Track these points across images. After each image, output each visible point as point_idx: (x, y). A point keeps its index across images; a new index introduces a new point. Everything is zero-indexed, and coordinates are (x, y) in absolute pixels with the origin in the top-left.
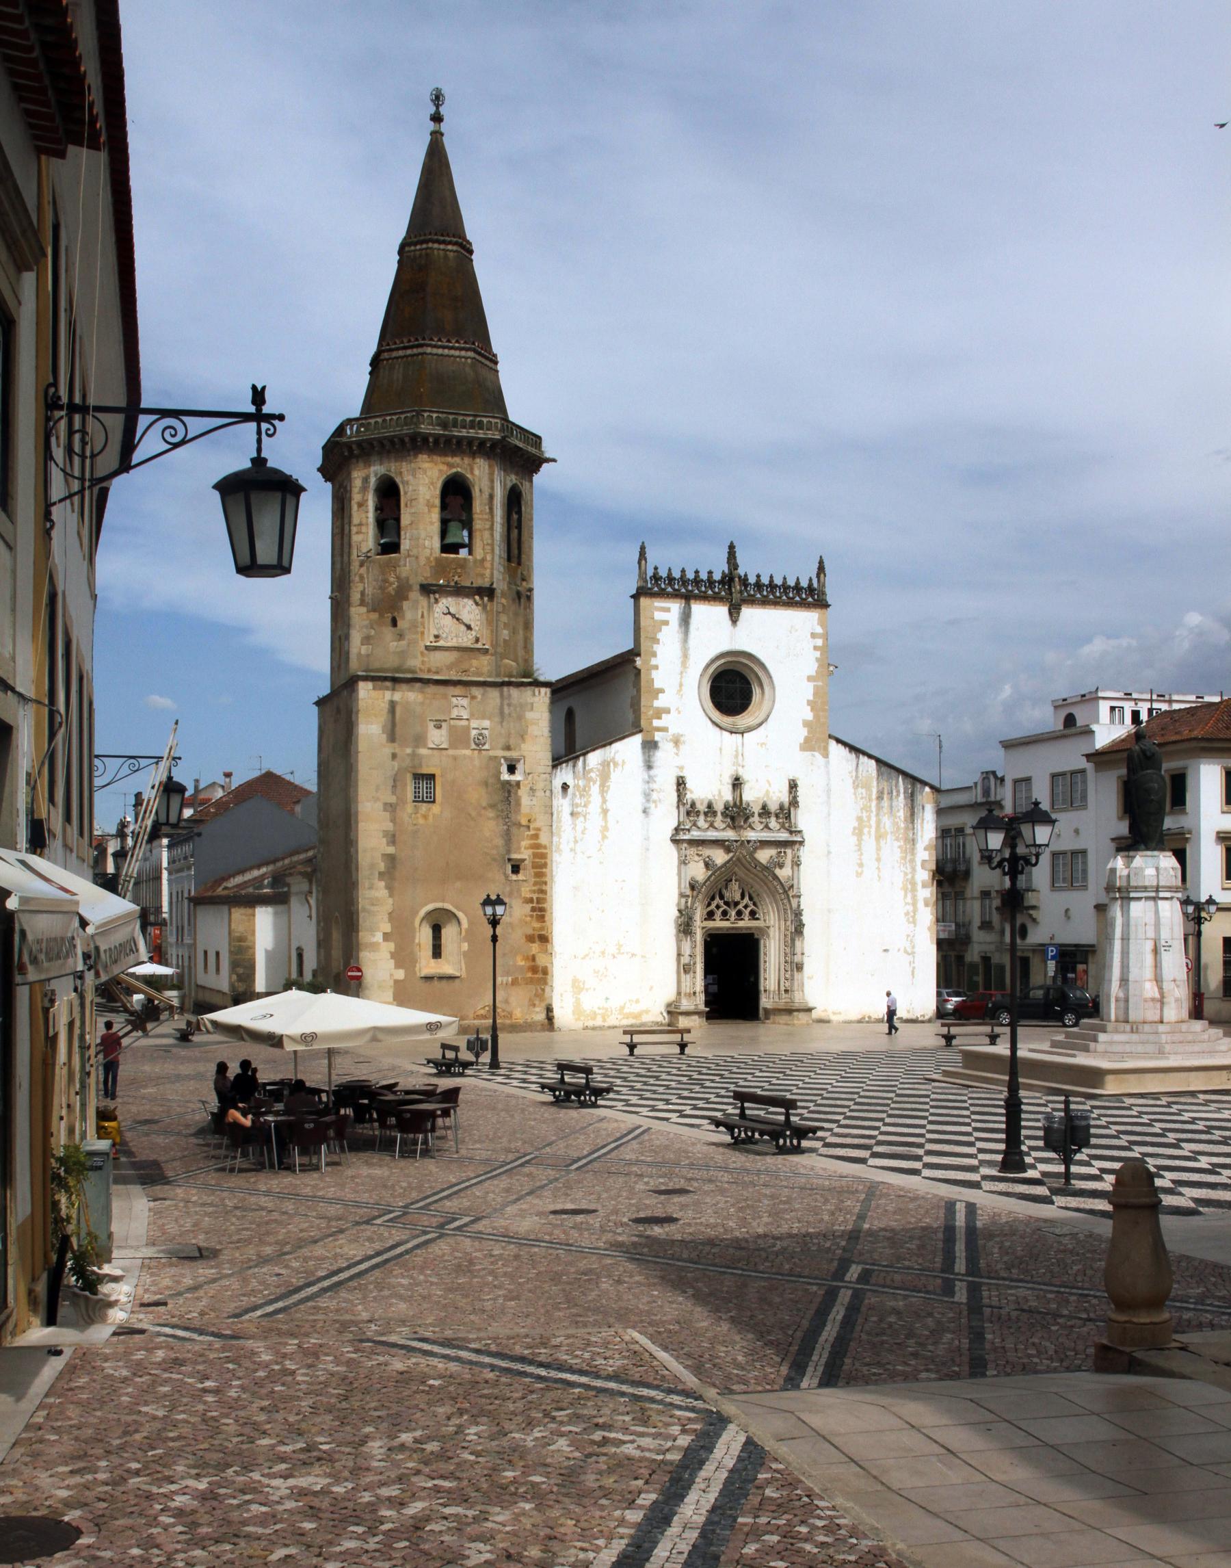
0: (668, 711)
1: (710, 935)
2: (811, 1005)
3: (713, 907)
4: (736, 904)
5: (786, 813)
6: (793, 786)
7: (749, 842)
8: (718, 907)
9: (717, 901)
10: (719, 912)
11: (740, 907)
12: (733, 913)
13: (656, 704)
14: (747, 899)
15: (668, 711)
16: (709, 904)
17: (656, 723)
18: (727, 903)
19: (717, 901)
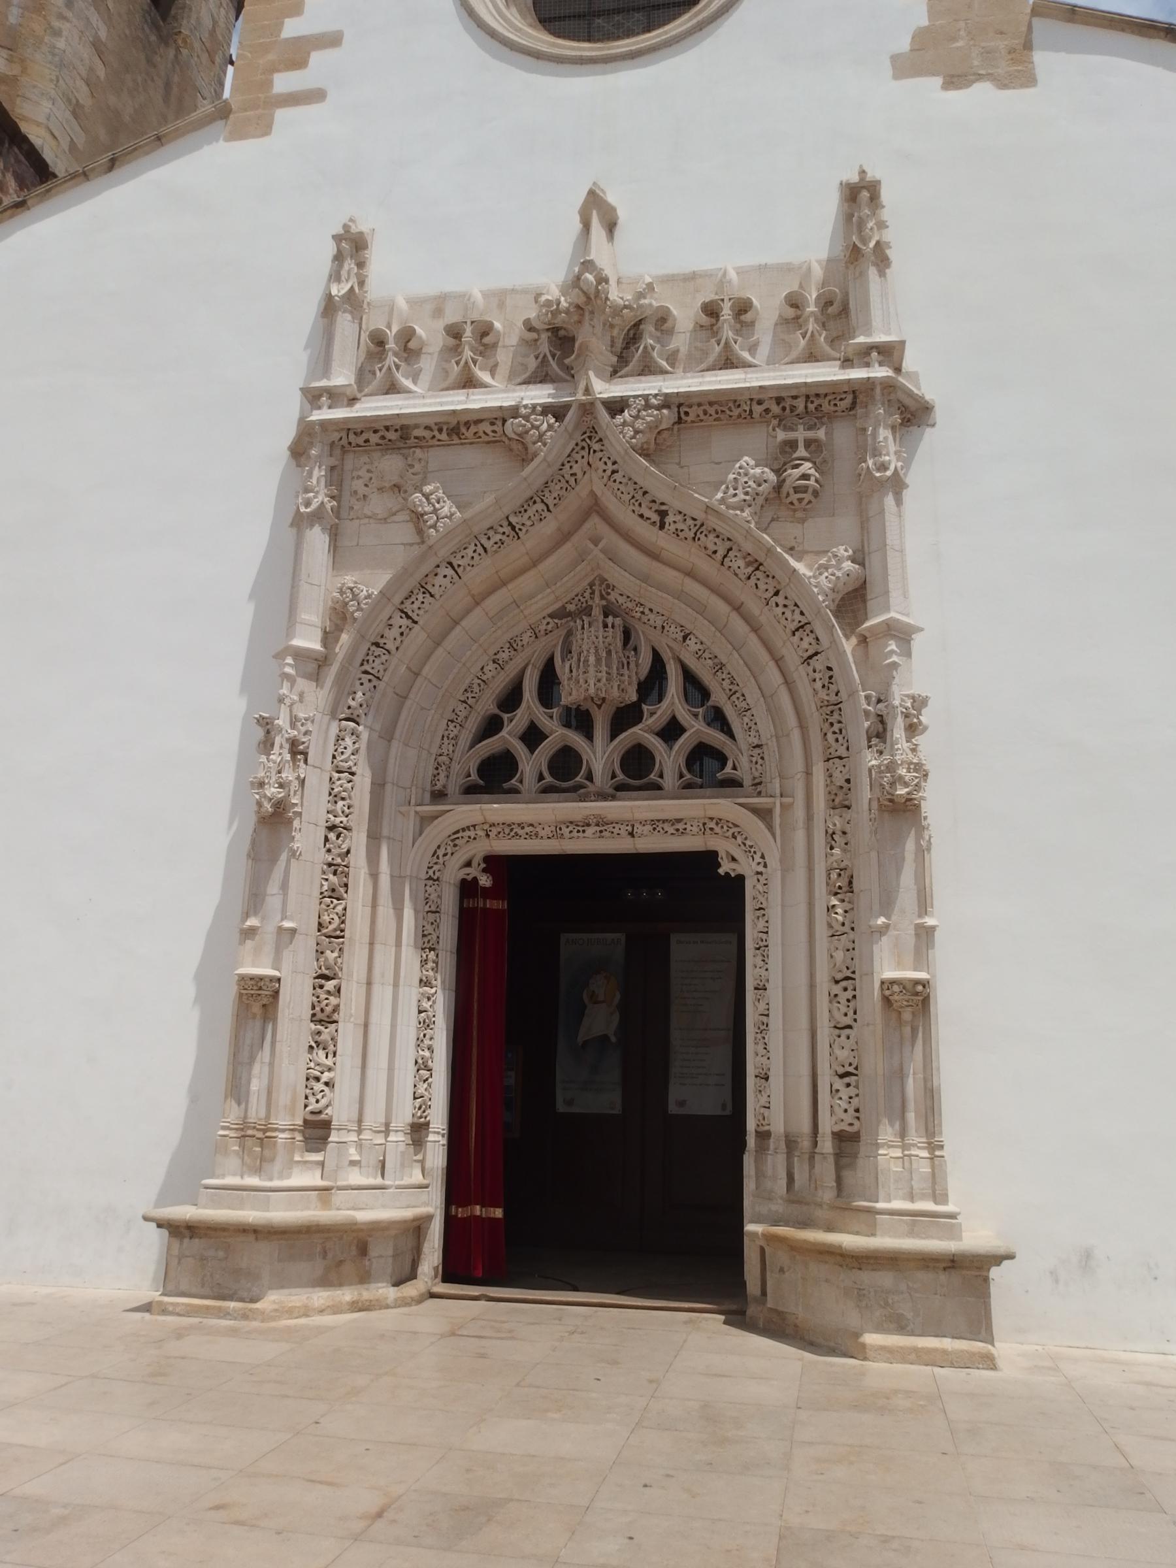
0: (332, 40)
1: (493, 863)
2: (975, 1237)
3: (509, 737)
4: (625, 717)
5: (833, 312)
6: (860, 196)
7: (616, 407)
8: (533, 736)
9: (530, 707)
10: (531, 764)
11: (642, 733)
12: (600, 755)
13: (292, 28)
14: (673, 701)
15: (332, 40)
16: (492, 726)
17: (284, 82)
18: (580, 720)
19: (530, 707)
